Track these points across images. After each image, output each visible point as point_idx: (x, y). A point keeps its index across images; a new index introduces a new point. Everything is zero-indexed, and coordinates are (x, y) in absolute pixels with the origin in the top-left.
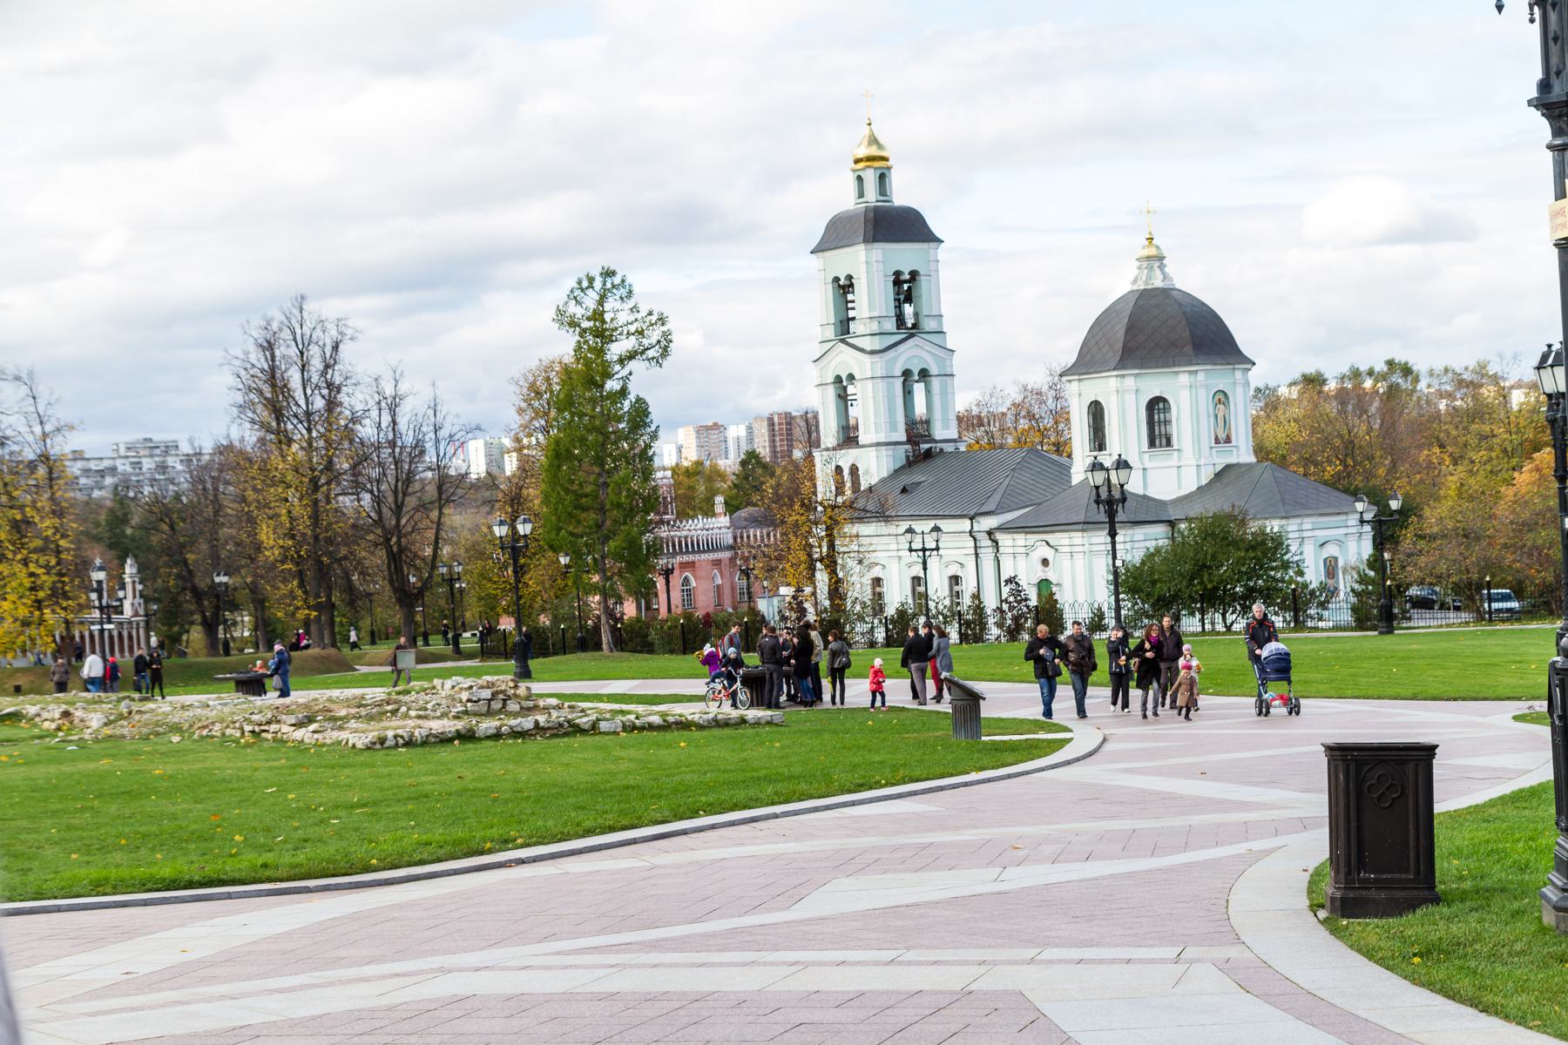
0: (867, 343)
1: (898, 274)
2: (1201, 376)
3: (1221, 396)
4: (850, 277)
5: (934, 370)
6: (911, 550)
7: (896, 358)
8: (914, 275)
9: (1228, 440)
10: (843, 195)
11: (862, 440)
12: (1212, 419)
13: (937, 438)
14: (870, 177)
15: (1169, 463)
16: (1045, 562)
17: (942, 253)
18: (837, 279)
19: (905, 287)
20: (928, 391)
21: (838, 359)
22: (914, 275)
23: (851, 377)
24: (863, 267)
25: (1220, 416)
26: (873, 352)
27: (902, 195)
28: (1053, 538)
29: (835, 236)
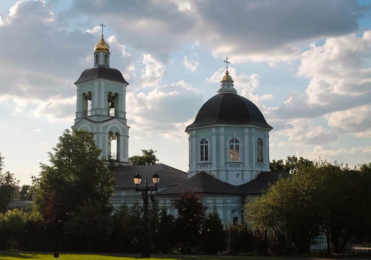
1: (110, 93)
2: (253, 130)
3: (259, 141)
4: (90, 92)
5: (121, 134)
7: (107, 126)
8: (116, 94)
9: (262, 161)
10: (89, 63)
12: (257, 151)
13: (121, 161)
14: (102, 56)
15: (238, 169)
17: (128, 87)
18: (84, 94)
20: (118, 143)
21: (82, 125)
22: (116, 94)
24: (96, 89)
25: (259, 149)
27: (113, 65)
29: (86, 76)
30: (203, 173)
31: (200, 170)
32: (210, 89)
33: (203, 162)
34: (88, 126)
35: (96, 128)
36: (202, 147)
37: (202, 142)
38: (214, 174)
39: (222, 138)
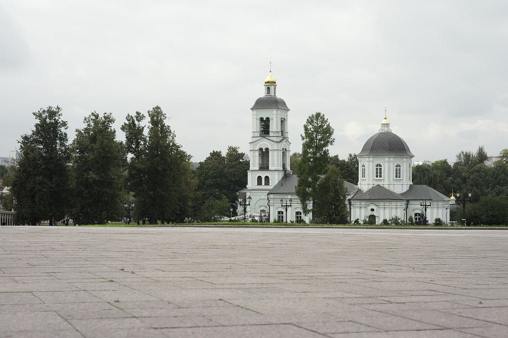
0: (275, 139)
6: (421, 205)
10: (262, 93)
11: (270, 168)
16: (372, 210)
19: (283, 121)
21: (261, 143)
23: (267, 149)
24: (275, 116)
26: (277, 142)
27: (279, 95)
28: (377, 203)
30: (378, 185)
31: (376, 183)
32: (375, 129)
33: (377, 178)
34: (267, 143)
35: (276, 146)
36: (377, 169)
37: (377, 166)
38: (386, 187)
39: (392, 164)
